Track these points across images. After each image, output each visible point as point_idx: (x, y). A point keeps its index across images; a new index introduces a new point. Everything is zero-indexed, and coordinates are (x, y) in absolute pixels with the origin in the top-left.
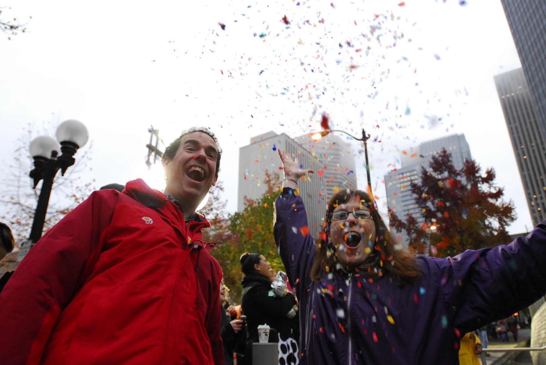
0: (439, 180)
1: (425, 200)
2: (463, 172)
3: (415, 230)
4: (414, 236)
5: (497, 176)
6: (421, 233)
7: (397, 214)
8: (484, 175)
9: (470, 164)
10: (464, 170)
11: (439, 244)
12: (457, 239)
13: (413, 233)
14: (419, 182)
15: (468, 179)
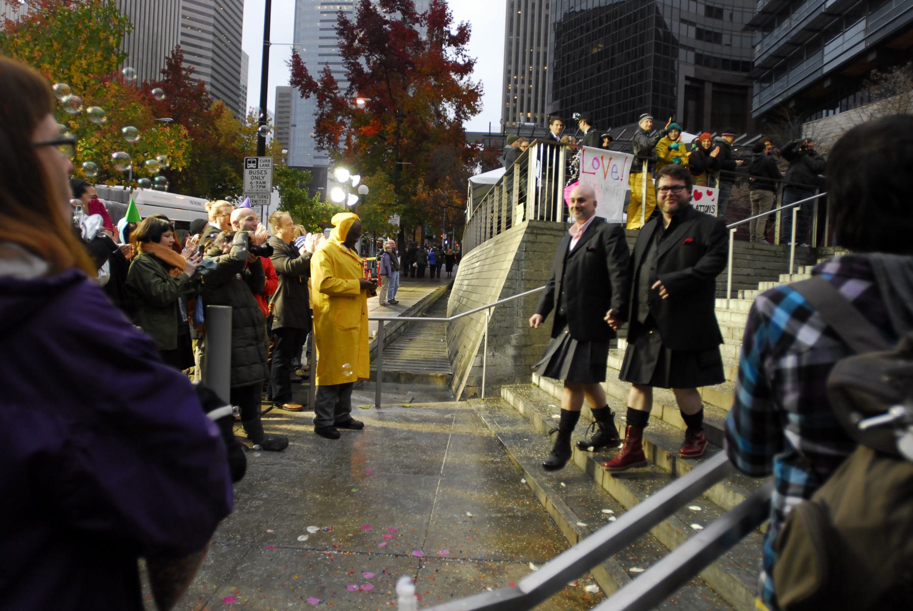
0: (386, 22)
1: (357, 52)
2: (425, 19)
3: (330, 97)
4: (328, 108)
5: (471, 38)
6: (340, 106)
7: (306, 66)
8: (454, 32)
9: (439, 8)
10: (427, 16)
11: (363, 129)
12: (391, 127)
13: (327, 103)
14: (353, 19)
15: (430, 32)
